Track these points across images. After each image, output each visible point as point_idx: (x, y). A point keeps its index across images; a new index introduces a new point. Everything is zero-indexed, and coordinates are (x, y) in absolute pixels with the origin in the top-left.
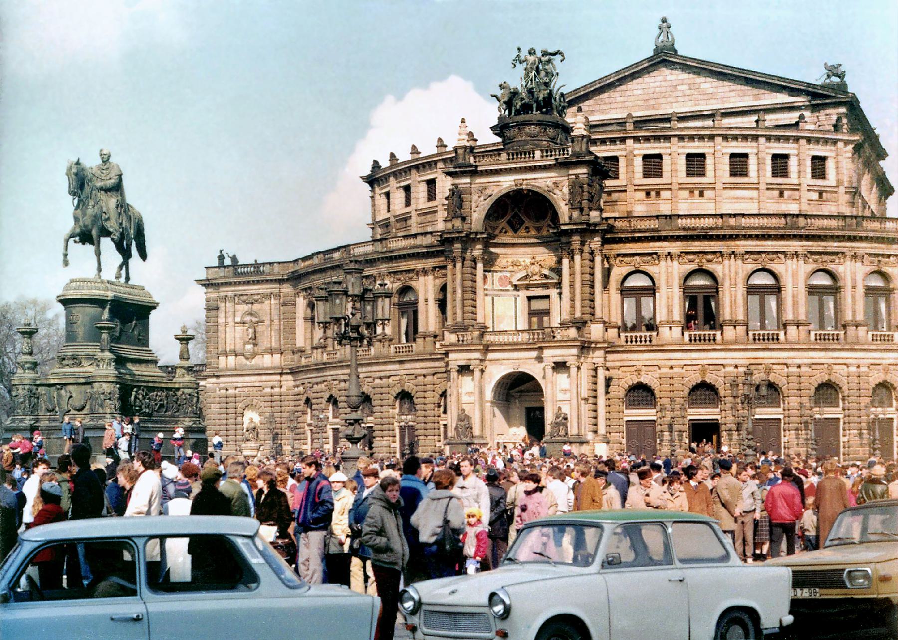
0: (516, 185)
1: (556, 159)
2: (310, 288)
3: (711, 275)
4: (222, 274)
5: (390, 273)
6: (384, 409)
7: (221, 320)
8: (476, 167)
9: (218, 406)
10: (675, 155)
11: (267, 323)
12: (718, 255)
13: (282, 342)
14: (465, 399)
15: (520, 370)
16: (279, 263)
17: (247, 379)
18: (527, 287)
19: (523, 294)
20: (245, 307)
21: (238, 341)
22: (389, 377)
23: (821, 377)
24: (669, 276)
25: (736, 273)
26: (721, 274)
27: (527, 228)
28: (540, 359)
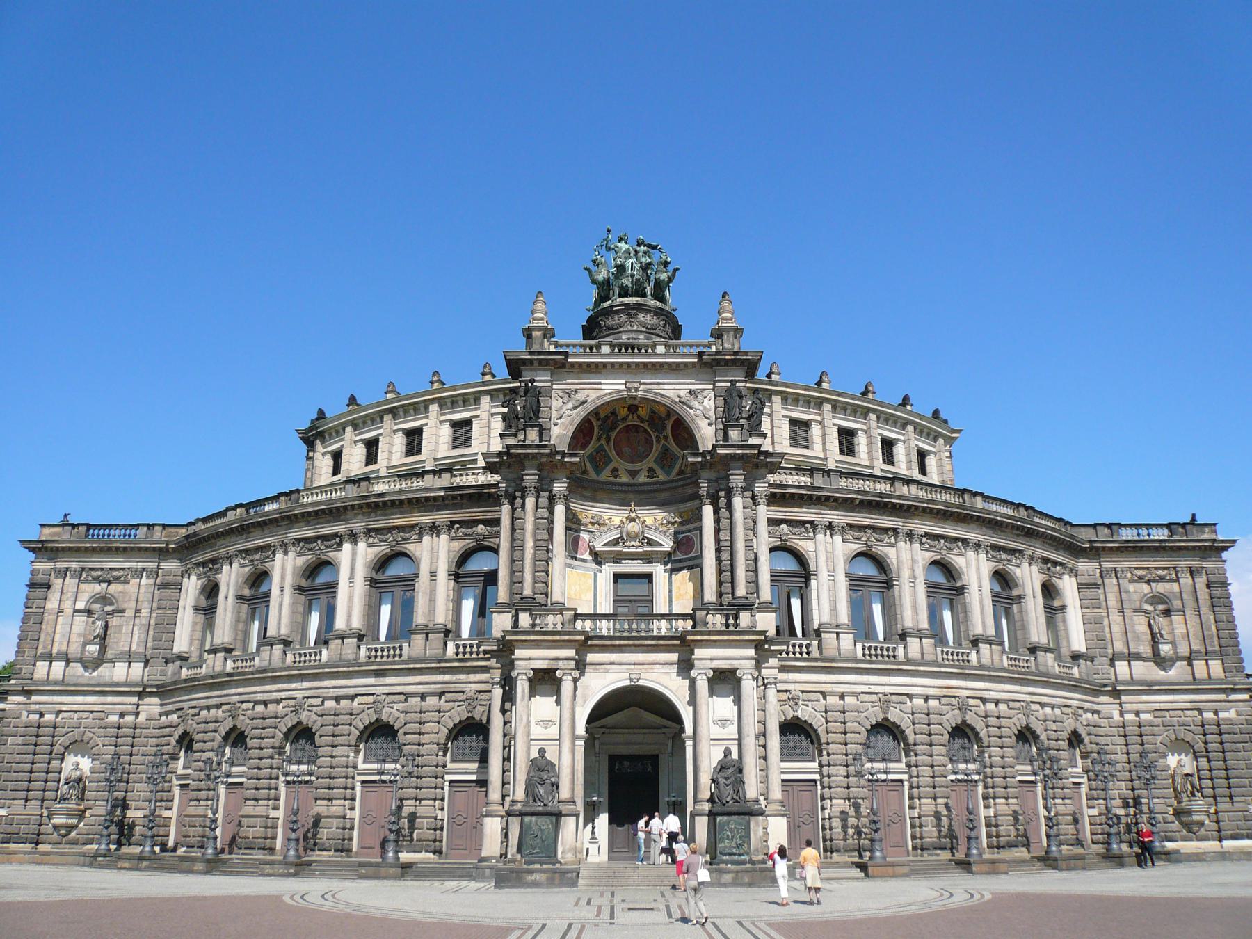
0: (628, 390)
1: (700, 354)
2: (214, 561)
3: (880, 563)
4: (66, 536)
5: (369, 531)
6: (339, 751)
7: (52, 604)
8: (566, 354)
9: (20, 740)
10: (776, 416)
11: (130, 613)
12: (890, 534)
13: (149, 645)
14: (537, 731)
15: (641, 683)
16: (164, 526)
17: (80, 699)
18: (617, 558)
19: (608, 570)
20: (98, 588)
21: (74, 638)
22: (353, 698)
23: (1019, 721)
24: (831, 556)
25: (914, 561)
26: (894, 561)
27: (615, 470)
28: (685, 666)
